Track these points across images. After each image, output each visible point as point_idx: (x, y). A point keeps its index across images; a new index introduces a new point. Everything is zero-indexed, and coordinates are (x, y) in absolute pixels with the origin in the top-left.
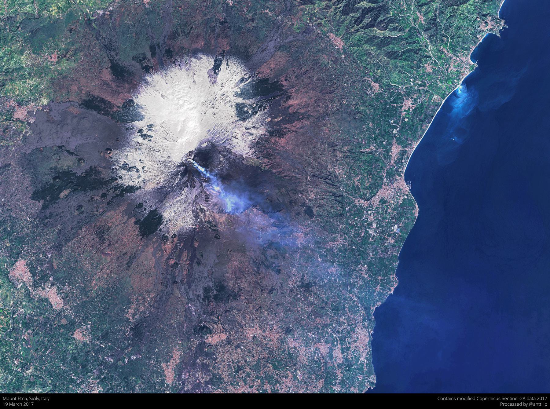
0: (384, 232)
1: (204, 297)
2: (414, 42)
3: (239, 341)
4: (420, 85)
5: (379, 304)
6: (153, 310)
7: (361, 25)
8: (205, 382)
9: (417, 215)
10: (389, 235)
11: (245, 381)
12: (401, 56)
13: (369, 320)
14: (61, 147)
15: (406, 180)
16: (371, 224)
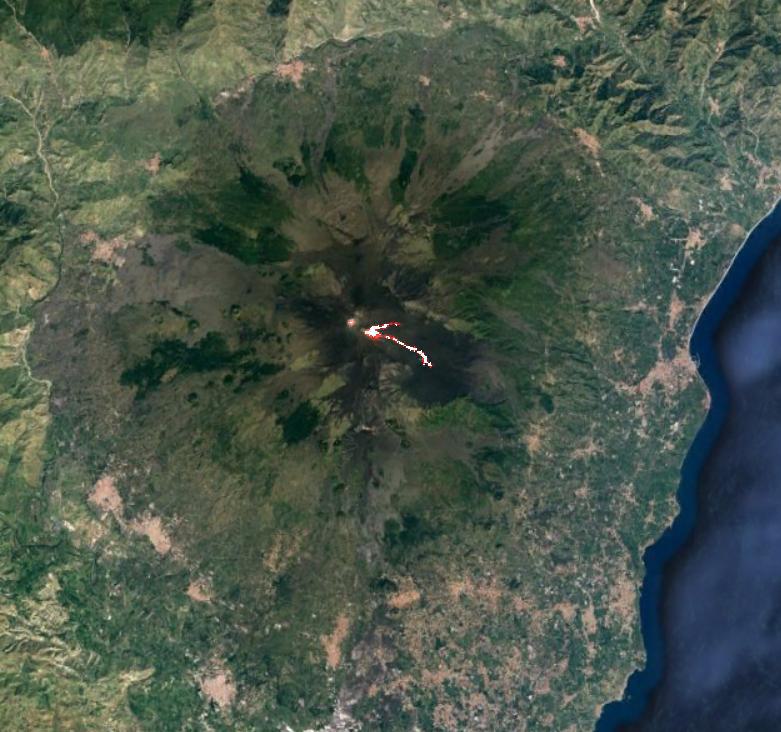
0: (659, 430)
1: (386, 536)
2: (705, 144)
3: (439, 602)
4: (714, 210)
5: (651, 542)
6: (307, 555)
7: (626, 116)
8: (388, 664)
9: (708, 407)
10: (667, 438)
11: (448, 662)
12: (687, 164)
13: (637, 567)
14: (164, 303)
15: (693, 353)
16: (638, 421)
